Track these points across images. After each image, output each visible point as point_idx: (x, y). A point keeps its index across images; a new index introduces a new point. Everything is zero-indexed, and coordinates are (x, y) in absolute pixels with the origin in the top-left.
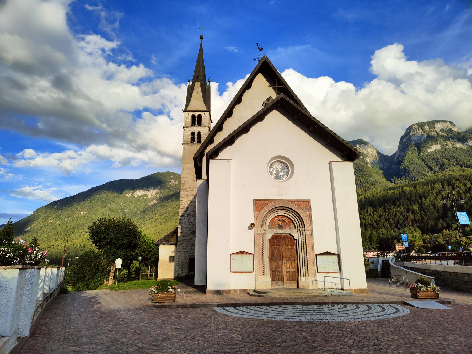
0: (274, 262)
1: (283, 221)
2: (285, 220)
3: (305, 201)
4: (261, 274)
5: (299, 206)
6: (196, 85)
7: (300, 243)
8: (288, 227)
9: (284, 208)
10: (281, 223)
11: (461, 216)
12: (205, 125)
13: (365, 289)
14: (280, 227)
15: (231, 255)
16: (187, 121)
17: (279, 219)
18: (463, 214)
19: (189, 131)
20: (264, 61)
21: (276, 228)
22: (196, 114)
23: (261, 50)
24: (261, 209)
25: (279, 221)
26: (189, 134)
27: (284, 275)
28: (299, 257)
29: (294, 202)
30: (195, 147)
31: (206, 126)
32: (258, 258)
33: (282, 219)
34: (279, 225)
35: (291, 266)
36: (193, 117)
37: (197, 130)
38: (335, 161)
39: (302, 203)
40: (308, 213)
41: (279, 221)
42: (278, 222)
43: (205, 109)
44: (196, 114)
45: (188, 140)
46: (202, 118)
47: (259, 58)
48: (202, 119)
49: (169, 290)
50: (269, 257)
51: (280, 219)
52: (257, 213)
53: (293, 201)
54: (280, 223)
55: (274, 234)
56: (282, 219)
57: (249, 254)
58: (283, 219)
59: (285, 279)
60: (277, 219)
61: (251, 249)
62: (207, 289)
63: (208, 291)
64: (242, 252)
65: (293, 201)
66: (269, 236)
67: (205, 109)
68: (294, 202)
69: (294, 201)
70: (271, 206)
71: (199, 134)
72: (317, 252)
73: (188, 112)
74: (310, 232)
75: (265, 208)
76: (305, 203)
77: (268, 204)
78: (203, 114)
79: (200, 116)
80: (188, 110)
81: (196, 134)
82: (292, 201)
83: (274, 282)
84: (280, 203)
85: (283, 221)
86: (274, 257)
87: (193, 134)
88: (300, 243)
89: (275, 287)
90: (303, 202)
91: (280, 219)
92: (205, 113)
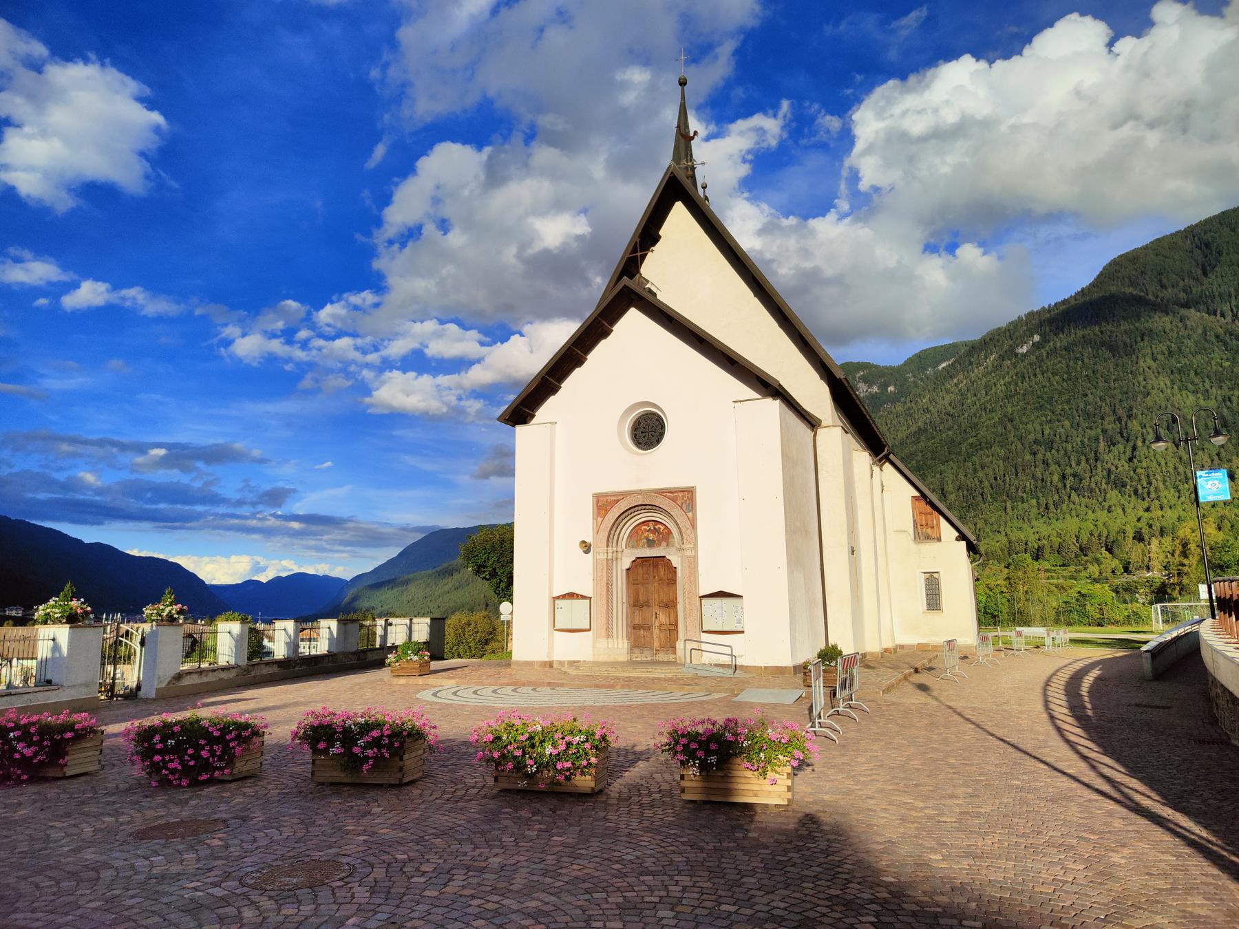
0: (637, 612)
1: (655, 531)
2: (660, 528)
4: (604, 632)
5: (674, 500)
8: (664, 544)
9: (650, 507)
11: (1207, 481)
13: (786, 667)
14: (651, 543)
18: (1217, 474)
21: (643, 547)
24: (607, 512)
27: (655, 637)
32: (599, 606)
33: (655, 528)
34: (648, 539)
35: (668, 620)
38: (740, 401)
39: (681, 494)
49: (409, 658)
52: (600, 519)
54: (651, 537)
56: (655, 528)
57: (583, 597)
59: (656, 644)
61: (586, 588)
64: (571, 595)
66: (626, 563)
70: (623, 505)
72: (701, 594)
74: (693, 551)
75: (614, 509)
77: (618, 501)
82: (661, 492)
83: (636, 650)
84: (640, 497)
85: (655, 531)
86: (637, 603)
89: (639, 659)
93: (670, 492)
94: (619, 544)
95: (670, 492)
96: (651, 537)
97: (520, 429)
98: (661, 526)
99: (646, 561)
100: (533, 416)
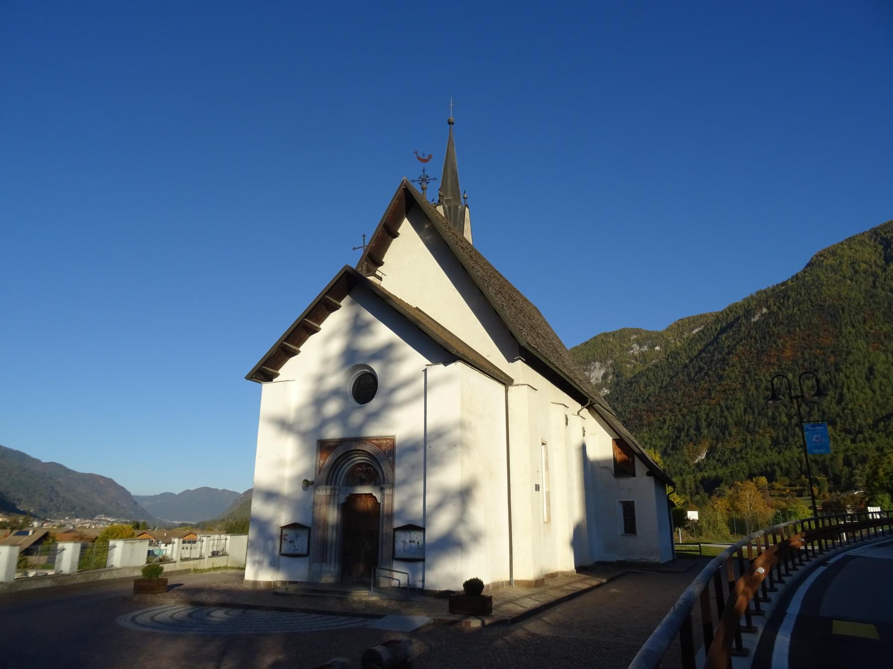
2: (370, 470)
9: (361, 452)
17: (361, 469)
25: (361, 472)
29: (373, 441)
41: (361, 472)
42: (360, 474)
47: (428, 179)
53: (371, 440)
54: (363, 476)
58: (368, 469)
60: (359, 468)
65: (371, 440)
68: (373, 441)
90: (386, 439)
91: (363, 470)
93: (377, 440)
94: (337, 482)
95: (377, 440)
96: (363, 476)
97: (266, 387)
99: (358, 497)
100: (277, 375)
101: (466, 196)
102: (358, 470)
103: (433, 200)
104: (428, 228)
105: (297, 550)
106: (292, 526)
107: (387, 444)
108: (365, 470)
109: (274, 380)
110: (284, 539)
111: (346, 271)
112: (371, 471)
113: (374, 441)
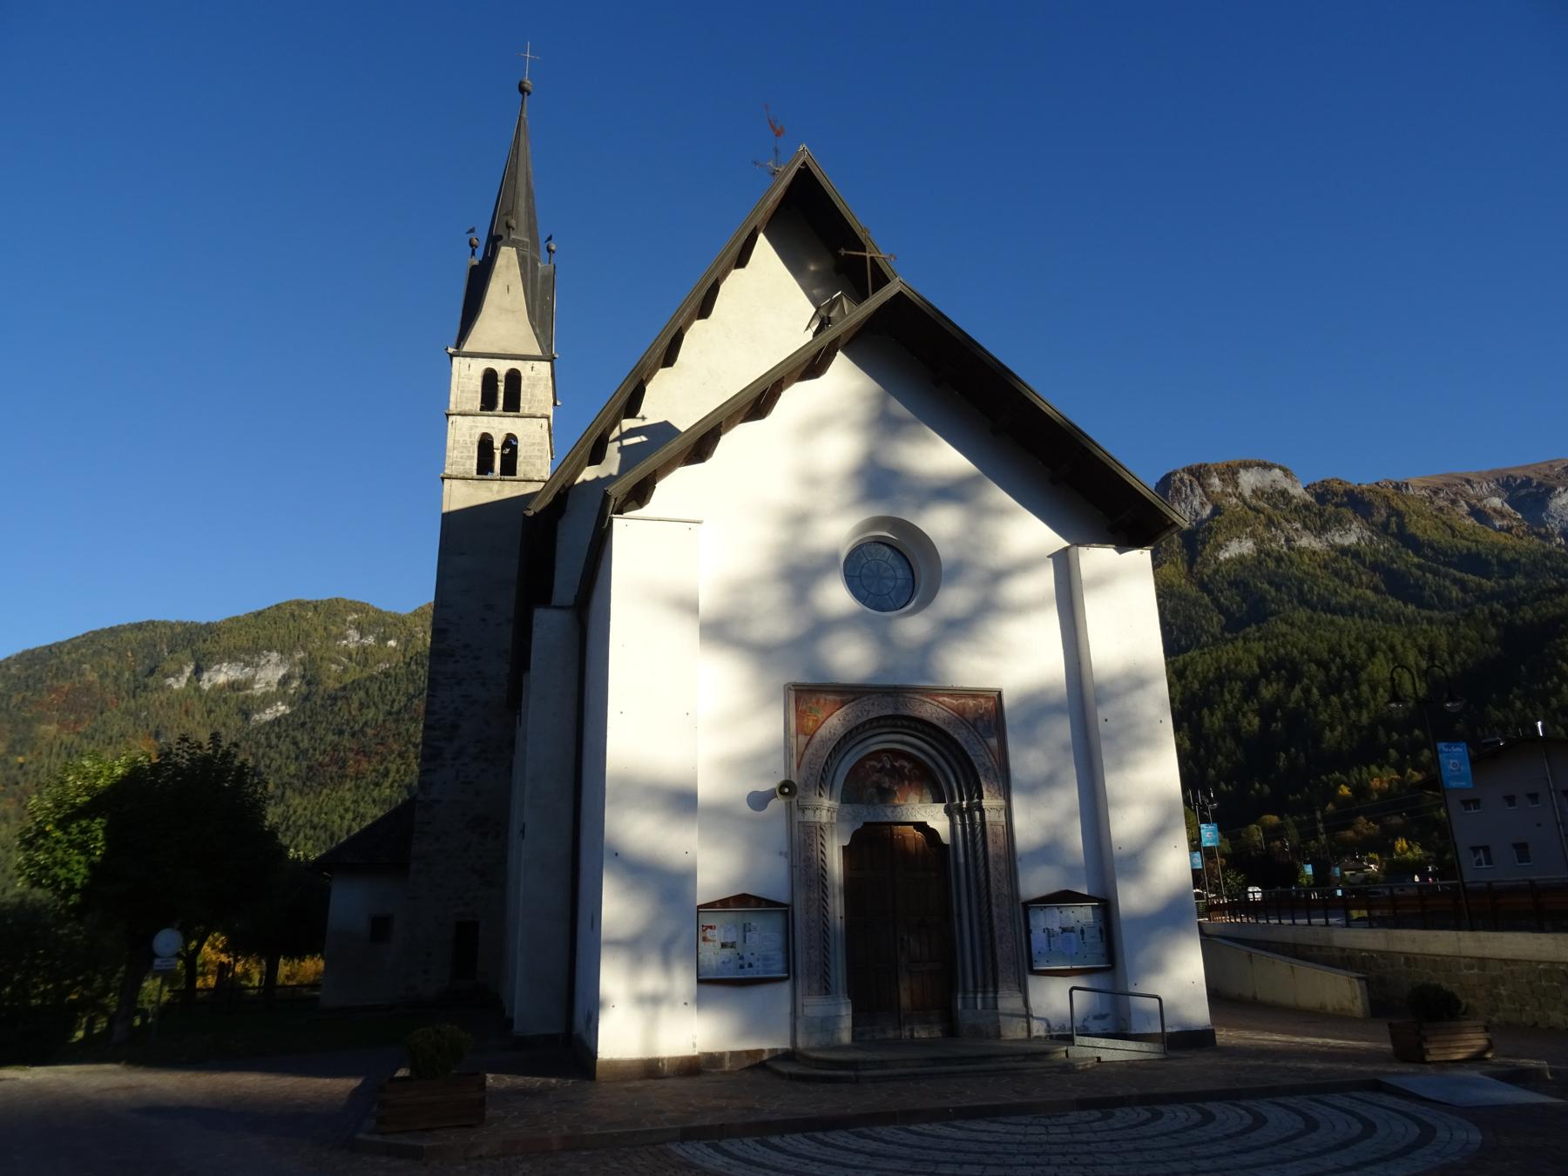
2: (903, 767)
3: (982, 696)
6: (501, 261)
7: (962, 859)
10: (887, 779)
12: (533, 411)
15: (698, 912)
16: (462, 392)
17: (879, 766)
19: (471, 428)
20: (799, 169)
22: (502, 367)
23: (778, 135)
26: (468, 440)
28: (960, 915)
29: (941, 699)
30: (491, 491)
31: (539, 415)
36: (490, 377)
37: (500, 427)
40: (993, 742)
42: (876, 777)
43: (537, 351)
44: (502, 367)
45: (464, 465)
46: (524, 383)
48: (523, 388)
50: (843, 916)
51: (883, 767)
55: (864, 823)
56: (892, 765)
58: (897, 764)
60: (873, 763)
62: (600, 1056)
63: (613, 1065)
65: (938, 695)
67: (537, 351)
68: (941, 699)
69: (943, 695)
71: (510, 442)
73: (468, 359)
76: (982, 701)
78: (524, 368)
79: (514, 378)
80: (467, 348)
81: (497, 444)
87: (485, 443)
88: (962, 859)
91: (883, 767)
92: (536, 364)
95: (950, 696)
98: (905, 764)
101: (553, 248)
102: (871, 766)
103: (472, 231)
104: (814, 271)
105: (750, 965)
106: (740, 902)
107: (977, 708)
108: (888, 766)
109: (626, 515)
110: (705, 939)
111: (900, 292)
112: (906, 770)
113: (946, 699)
